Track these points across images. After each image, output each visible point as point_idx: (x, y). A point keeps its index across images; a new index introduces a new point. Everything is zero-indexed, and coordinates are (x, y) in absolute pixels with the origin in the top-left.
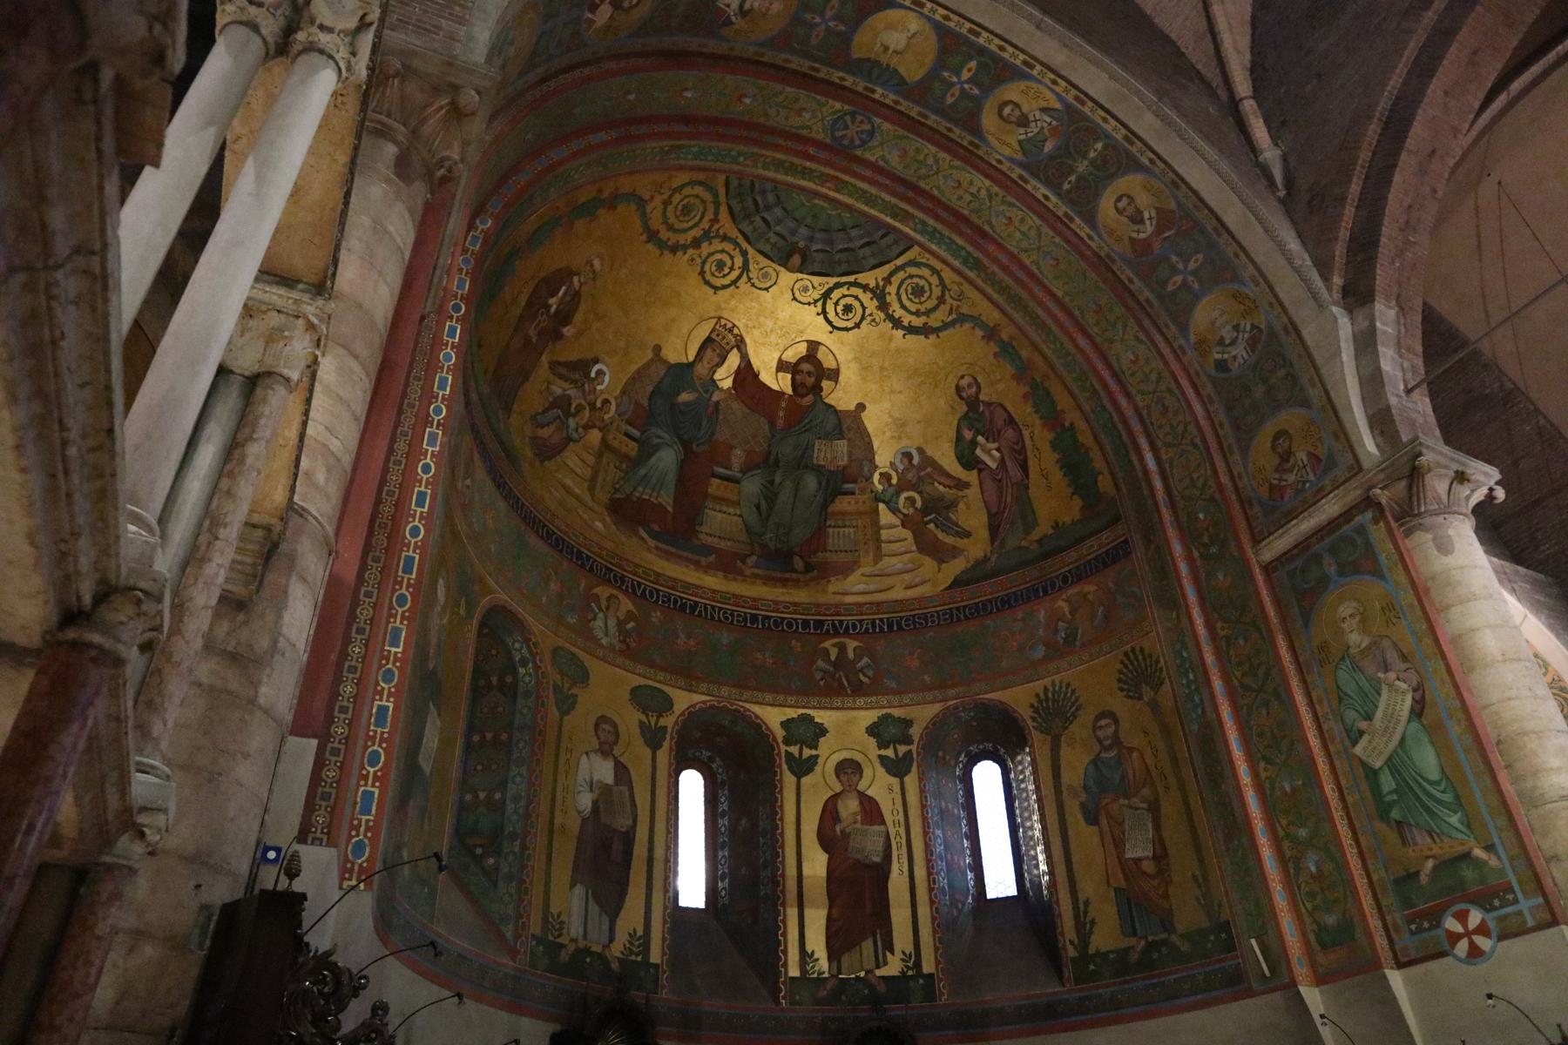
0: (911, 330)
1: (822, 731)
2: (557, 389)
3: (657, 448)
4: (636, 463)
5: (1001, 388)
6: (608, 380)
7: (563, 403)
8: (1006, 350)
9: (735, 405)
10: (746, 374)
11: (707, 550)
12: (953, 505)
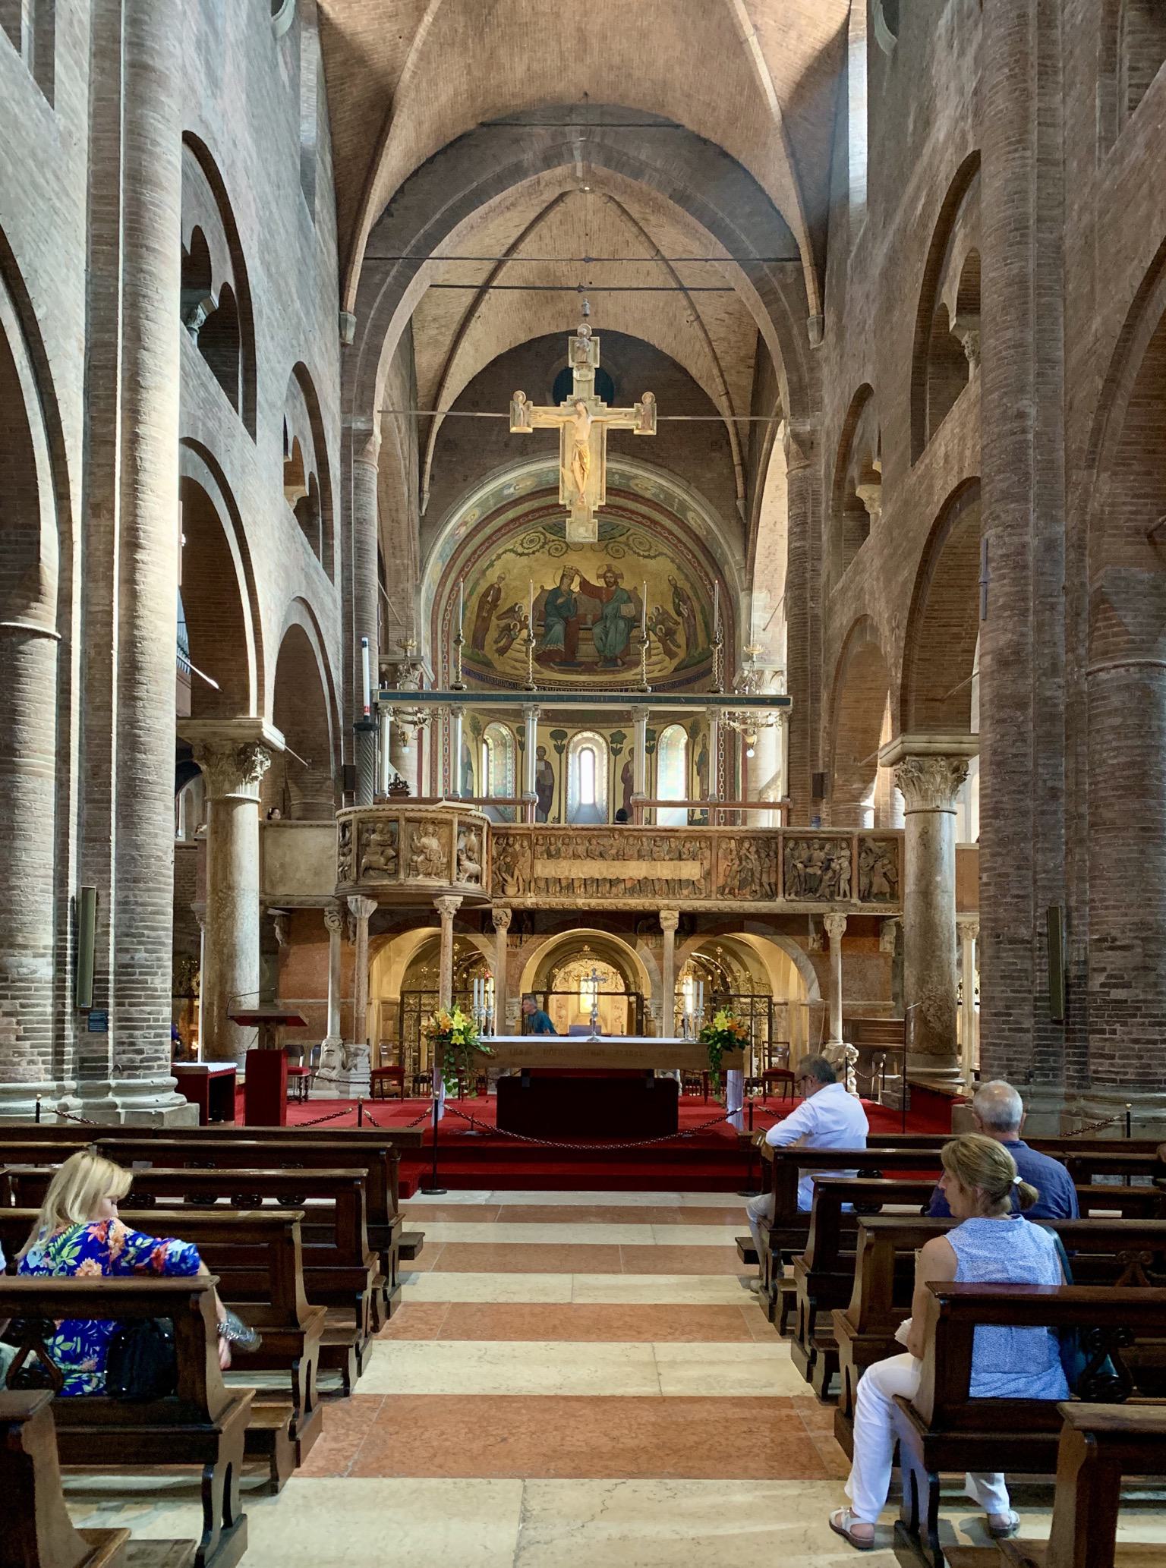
0: (645, 557)
1: (625, 737)
2: (503, 623)
3: (552, 626)
4: (544, 636)
5: (682, 583)
6: (527, 610)
7: (507, 628)
8: (679, 568)
9: (584, 597)
10: (584, 584)
11: (580, 664)
12: (675, 633)
